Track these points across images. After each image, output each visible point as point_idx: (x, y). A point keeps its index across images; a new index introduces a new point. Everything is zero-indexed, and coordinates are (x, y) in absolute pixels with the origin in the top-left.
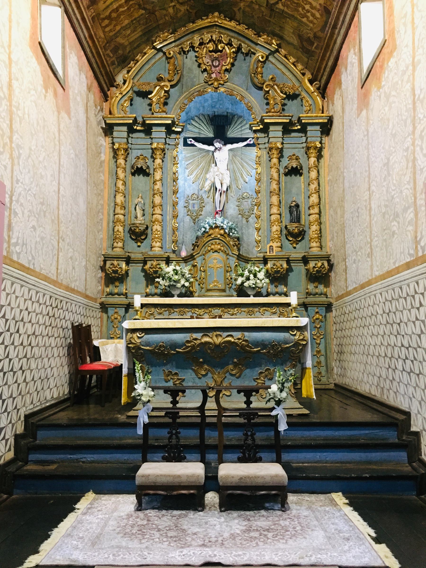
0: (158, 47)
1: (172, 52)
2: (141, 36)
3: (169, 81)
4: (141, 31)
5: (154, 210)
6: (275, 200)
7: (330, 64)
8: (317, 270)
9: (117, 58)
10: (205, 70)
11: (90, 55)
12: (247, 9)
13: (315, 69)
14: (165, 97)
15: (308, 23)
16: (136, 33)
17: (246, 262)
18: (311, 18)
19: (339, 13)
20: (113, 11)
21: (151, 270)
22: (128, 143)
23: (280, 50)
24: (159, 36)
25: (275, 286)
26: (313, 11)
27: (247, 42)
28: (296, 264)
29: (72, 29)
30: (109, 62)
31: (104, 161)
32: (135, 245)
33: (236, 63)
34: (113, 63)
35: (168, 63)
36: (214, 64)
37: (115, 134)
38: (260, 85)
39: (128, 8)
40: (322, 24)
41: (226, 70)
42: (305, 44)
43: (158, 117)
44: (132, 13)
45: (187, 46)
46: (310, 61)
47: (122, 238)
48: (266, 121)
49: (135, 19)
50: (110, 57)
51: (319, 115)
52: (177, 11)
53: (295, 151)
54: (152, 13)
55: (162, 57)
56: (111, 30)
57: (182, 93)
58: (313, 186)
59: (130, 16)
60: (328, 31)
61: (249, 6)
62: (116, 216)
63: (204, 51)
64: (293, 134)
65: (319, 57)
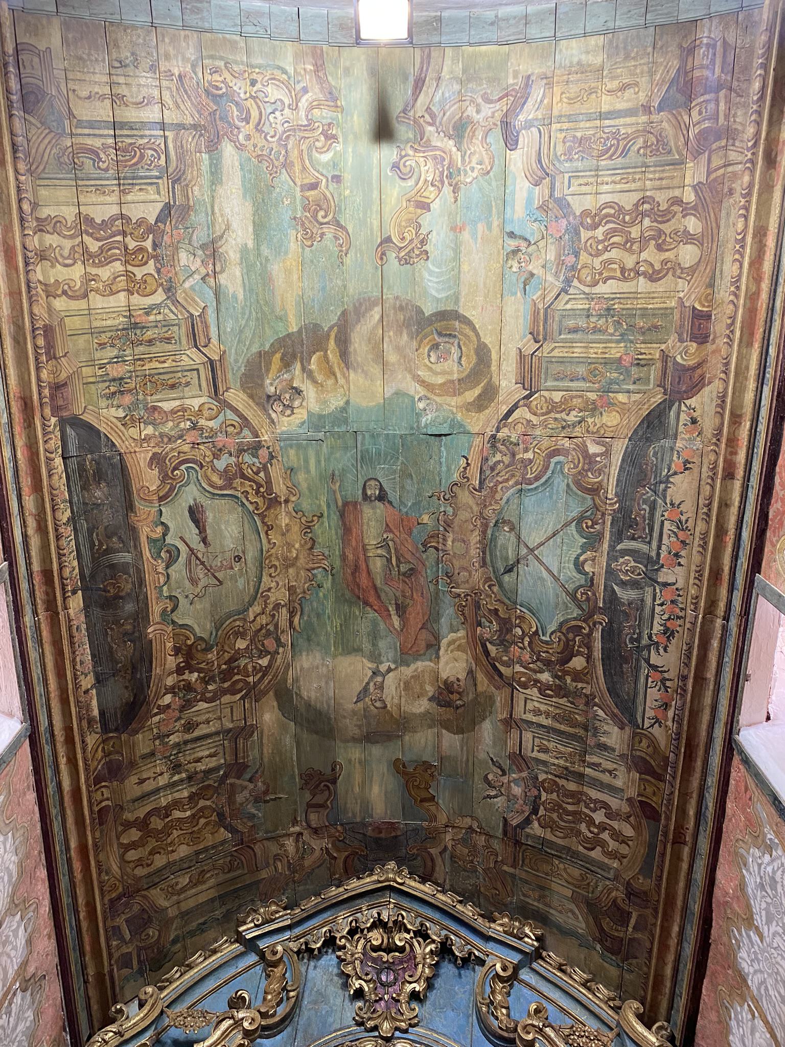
0: (248, 937)
1: (279, 948)
2: (212, 900)
3: (264, 1015)
7: (689, 950)
9: (139, 949)
10: (359, 994)
11: (65, 900)
12: (462, 850)
13: (646, 984)
15: (606, 861)
18: (612, 845)
19: (684, 795)
20: (155, 811)
23: (544, 954)
26: (615, 824)
27: (463, 932)
29: (32, 796)
30: (116, 955)
33: (438, 983)
34: (125, 962)
35: (268, 976)
36: (384, 978)
38: (505, 1034)
39: (193, 816)
40: (643, 850)
41: (414, 996)
42: (606, 923)
44: (200, 831)
46: (627, 976)
49: (206, 849)
50: (122, 938)
52: (303, 851)
54: (245, 844)
55: (253, 966)
56: (140, 859)
59: (195, 837)
60: (663, 855)
61: (464, 841)
63: (360, 947)
65: (652, 943)
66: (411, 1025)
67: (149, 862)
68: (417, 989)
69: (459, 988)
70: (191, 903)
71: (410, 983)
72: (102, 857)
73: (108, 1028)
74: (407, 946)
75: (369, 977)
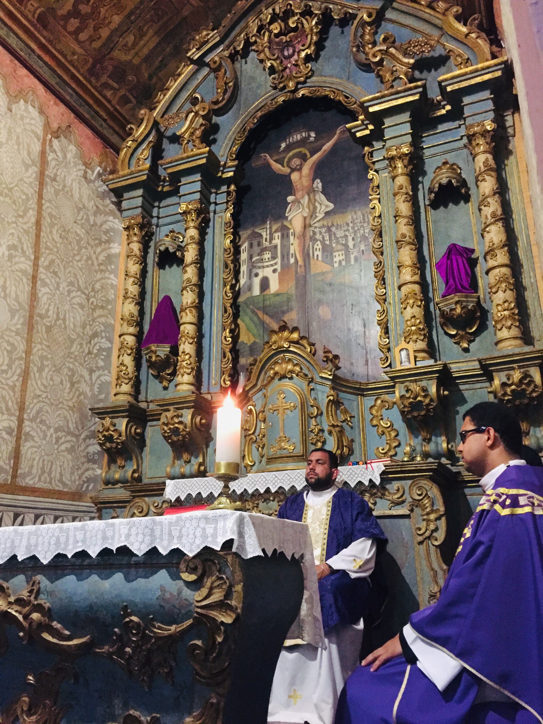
0: (196, 58)
1: (217, 59)
2: (159, 43)
4: (156, 33)
5: (181, 317)
6: (407, 255)
8: (513, 391)
9: (130, 91)
14: (203, 128)
16: (145, 39)
17: (357, 395)
21: (166, 428)
22: (152, 217)
24: (194, 39)
25: (424, 440)
28: (471, 386)
31: (119, 255)
32: (160, 386)
33: (327, 44)
35: (217, 78)
36: (286, 53)
37: (125, 205)
41: (308, 59)
43: (183, 159)
45: (240, 42)
47: (130, 375)
48: (371, 110)
51: (480, 66)
53: (451, 158)
55: (208, 74)
57: (236, 119)
58: (488, 211)
62: (122, 338)
64: (441, 128)
66: (307, 78)
67: (98, 36)
68: (309, 53)
69: (340, 41)
70: (146, 51)
71: (304, 50)
72: (58, 47)
73: (128, 139)
74: (299, 25)
75: (276, 56)
